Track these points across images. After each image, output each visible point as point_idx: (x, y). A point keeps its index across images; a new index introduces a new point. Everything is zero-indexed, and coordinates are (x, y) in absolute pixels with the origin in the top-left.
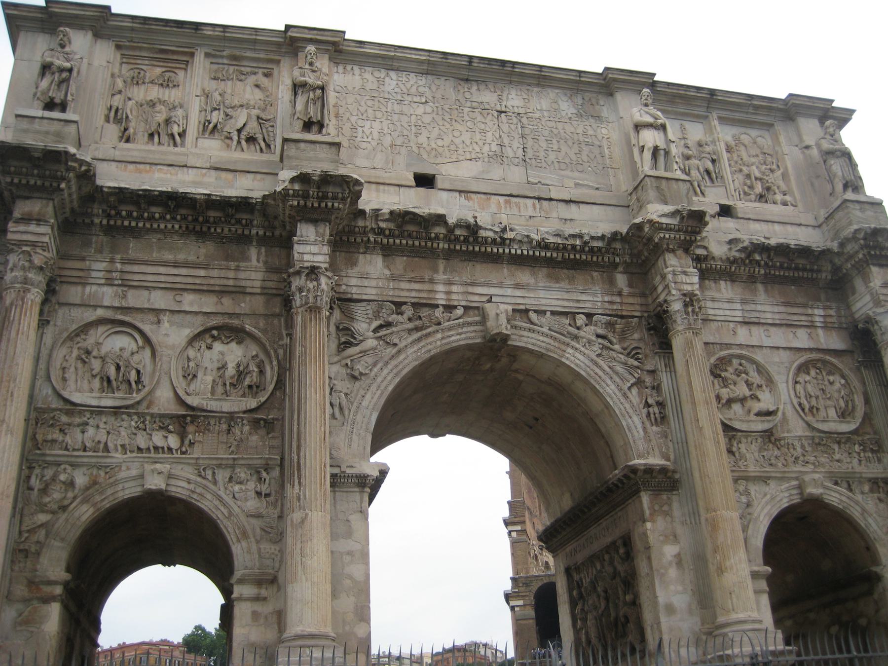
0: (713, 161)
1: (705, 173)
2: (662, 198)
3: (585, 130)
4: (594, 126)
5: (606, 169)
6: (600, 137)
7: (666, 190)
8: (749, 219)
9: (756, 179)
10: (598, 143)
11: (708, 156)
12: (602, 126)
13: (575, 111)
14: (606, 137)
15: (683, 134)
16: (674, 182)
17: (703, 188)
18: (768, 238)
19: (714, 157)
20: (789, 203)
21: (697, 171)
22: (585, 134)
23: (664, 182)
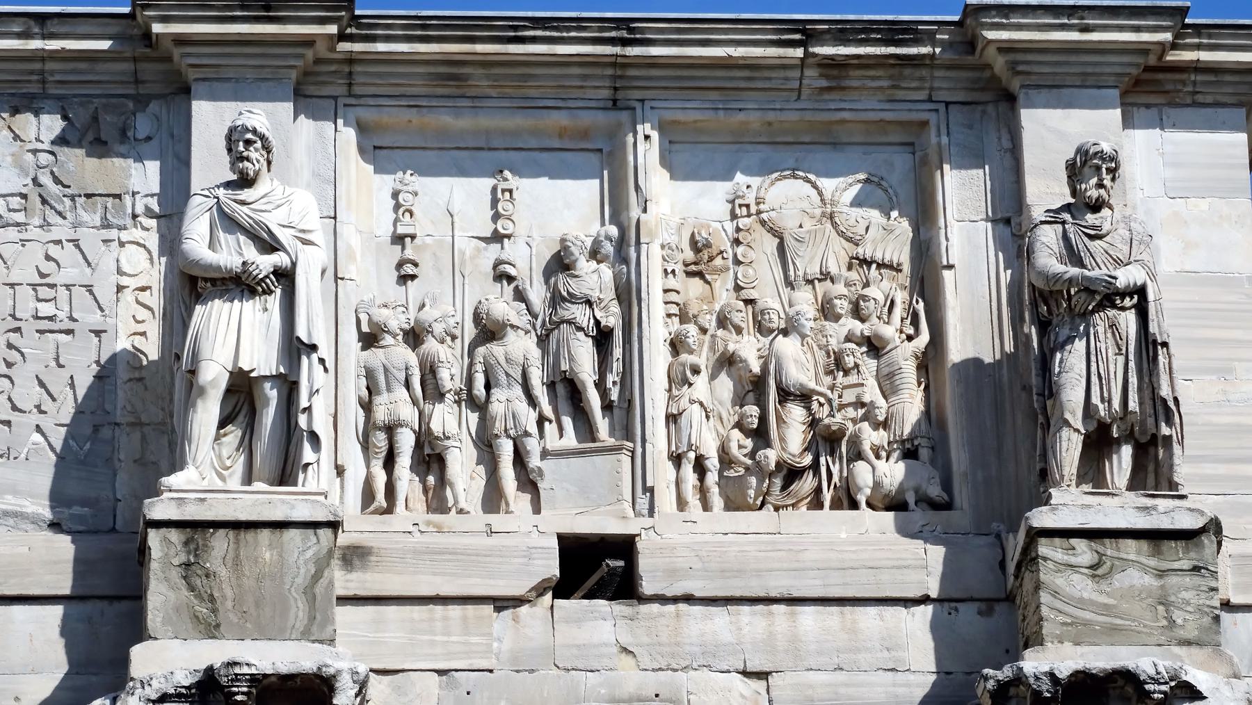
0: (602, 338)
1: (561, 389)
2: (203, 610)
3: (48, 267)
4: (90, 238)
5: (106, 433)
6: (105, 293)
7: (223, 572)
8: (689, 599)
9: (785, 395)
10: (95, 319)
11: (580, 314)
12: (125, 236)
13: (18, 183)
14: (132, 283)
15: (496, 217)
16: (265, 534)
17: (534, 461)
18: (762, 675)
19: (612, 318)
20: (911, 498)
21: (518, 391)
22: (43, 281)
23: (220, 542)
